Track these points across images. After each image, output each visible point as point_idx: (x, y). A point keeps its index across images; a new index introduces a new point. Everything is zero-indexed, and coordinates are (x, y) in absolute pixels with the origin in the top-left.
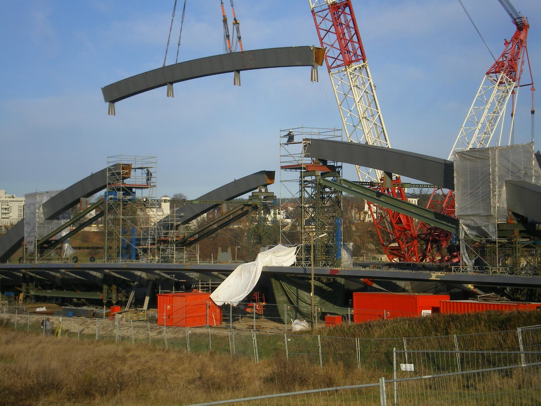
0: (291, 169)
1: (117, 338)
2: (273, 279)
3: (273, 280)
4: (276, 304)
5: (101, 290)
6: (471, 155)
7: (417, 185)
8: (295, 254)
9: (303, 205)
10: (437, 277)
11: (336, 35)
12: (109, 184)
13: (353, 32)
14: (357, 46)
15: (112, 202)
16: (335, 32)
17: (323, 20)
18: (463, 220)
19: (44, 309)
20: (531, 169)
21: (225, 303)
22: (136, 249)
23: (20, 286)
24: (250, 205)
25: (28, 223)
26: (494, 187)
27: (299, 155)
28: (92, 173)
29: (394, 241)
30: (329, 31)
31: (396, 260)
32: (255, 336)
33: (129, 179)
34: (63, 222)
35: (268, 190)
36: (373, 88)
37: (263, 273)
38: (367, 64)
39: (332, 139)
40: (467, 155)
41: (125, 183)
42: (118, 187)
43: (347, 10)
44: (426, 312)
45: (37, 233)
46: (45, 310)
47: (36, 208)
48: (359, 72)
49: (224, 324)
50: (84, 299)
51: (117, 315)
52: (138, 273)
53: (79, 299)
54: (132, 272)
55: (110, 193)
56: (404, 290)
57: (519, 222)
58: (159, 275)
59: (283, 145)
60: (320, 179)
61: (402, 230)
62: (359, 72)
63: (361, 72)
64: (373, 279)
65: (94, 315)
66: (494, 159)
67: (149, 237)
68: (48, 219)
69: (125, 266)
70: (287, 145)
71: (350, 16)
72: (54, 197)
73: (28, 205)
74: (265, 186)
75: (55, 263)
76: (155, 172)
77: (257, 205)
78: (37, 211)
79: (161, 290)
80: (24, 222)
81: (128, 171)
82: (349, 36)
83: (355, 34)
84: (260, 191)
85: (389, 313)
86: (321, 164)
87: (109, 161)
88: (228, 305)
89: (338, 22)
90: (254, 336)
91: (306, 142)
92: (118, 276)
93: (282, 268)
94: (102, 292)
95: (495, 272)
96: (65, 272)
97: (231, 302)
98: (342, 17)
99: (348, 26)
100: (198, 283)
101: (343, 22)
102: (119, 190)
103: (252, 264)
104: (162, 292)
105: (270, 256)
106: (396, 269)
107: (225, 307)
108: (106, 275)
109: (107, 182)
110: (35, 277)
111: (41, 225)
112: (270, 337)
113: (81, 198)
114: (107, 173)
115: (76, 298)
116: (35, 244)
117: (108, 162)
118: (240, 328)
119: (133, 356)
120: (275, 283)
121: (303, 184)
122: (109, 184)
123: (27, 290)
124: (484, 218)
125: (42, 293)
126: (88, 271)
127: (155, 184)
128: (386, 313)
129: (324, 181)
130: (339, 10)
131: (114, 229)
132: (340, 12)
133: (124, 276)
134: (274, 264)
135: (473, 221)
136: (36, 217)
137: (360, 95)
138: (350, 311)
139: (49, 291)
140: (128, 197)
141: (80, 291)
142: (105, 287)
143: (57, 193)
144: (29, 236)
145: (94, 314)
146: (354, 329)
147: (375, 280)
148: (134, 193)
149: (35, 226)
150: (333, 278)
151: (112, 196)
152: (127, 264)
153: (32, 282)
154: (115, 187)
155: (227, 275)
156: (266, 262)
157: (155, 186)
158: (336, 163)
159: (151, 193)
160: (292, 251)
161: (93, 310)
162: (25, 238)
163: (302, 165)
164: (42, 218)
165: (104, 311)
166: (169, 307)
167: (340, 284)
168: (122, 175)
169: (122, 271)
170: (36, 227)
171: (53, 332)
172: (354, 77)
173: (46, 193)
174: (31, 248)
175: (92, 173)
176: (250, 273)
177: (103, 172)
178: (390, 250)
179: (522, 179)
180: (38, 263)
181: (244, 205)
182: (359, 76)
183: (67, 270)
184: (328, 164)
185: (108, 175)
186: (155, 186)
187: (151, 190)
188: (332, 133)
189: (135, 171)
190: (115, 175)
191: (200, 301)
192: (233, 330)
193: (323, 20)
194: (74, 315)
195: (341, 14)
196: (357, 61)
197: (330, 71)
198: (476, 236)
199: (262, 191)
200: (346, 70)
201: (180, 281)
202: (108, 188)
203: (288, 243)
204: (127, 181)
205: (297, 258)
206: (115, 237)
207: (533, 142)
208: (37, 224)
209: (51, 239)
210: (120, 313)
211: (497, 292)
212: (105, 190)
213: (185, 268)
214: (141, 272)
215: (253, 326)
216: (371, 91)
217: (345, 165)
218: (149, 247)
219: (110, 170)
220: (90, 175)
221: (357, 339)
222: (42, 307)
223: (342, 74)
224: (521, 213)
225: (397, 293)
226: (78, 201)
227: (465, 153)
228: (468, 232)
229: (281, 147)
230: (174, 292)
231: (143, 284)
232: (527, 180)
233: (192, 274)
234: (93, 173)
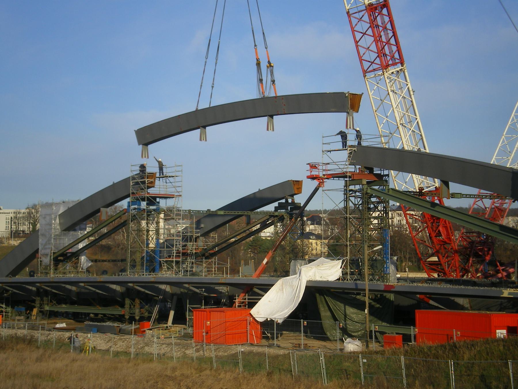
0: (334, 177)
1: (155, 356)
3: (317, 295)
4: (321, 320)
5: (122, 306)
7: (468, 195)
8: (341, 268)
9: (348, 215)
10: (510, 294)
11: (373, 38)
12: (133, 193)
13: (391, 34)
15: (136, 213)
16: (372, 35)
17: (359, 22)
19: (64, 325)
21: (267, 319)
22: (160, 261)
23: (34, 301)
24: (277, 216)
25: (43, 235)
27: (344, 163)
28: (114, 182)
29: (432, 255)
30: (365, 34)
31: (436, 275)
32: (323, 356)
33: (153, 188)
34: (80, 234)
35: (295, 200)
36: (412, 93)
37: (307, 288)
38: (405, 68)
39: (379, 146)
41: (149, 193)
42: (142, 197)
43: (385, 11)
44: (501, 333)
45: (53, 244)
46: (65, 326)
47: (52, 219)
48: (396, 76)
49: (264, 342)
50: (102, 314)
51: (147, 331)
52: (163, 287)
53: (96, 315)
54: (157, 285)
55: (133, 203)
56: (462, 308)
58: (188, 289)
59: (326, 152)
60: (367, 188)
61: (442, 243)
62: (396, 76)
63: (398, 77)
64: (431, 295)
65: (121, 332)
67: (174, 248)
68: (65, 230)
69: (153, 280)
70: (330, 152)
71: (388, 18)
72: (71, 207)
73: (43, 216)
74: (292, 196)
75: (71, 276)
76: (181, 181)
77: (283, 216)
78: (53, 222)
79: (189, 305)
80: (39, 234)
81: (153, 180)
82: (386, 39)
83: (393, 37)
85: (459, 333)
86: (367, 172)
87: (132, 170)
88: (272, 321)
89: (374, 24)
90: (321, 356)
91: (352, 149)
92: (143, 290)
93: (327, 282)
94: (124, 308)
96: (85, 286)
97: (275, 318)
98: (379, 19)
99: (385, 28)
100: (235, 298)
101: (380, 24)
102: (143, 200)
103: (296, 277)
104: (191, 307)
106: (451, 285)
107: (268, 324)
108: (128, 290)
109: (131, 191)
110: (51, 291)
112: (330, 356)
113: (102, 209)
114: (131, 182)
115: (93, 314)
116: (51, 256)
117: (131, 171)
118: (284, 346)
119: (183, 375)
120: (319, 298)
121: (347, 192)
122: (133, 193)
123: (41, 305)
125: (56, 310)
126: (107, 285)
127: (181, 194)
128: (456, 334)
129: (372, 190)
130: (376, 11)
131: (138, 240)
132: (377, 12)
133: (149, 291)
134: (318, 278)
136: (52, 228)
137: (397, 102)
138: (413, 331)
139: (64, 306)
140: (152, 207)
142: (128, 302)
143: (74, 204)
144: (46, 249)
145: (120, 330)
146: (435, 350)
147: (432, 296)
148: (159, 203)
149: (51, 238)
150: (380, 294)
151: (136, 206)
152: (155, 277)
153: (47, 296)
154: (140, 197)
155: (266, 291)
156: (310, 276)
157: (180, 196)
158: (382, 171)
159: (176, 203)
161: (119, 326)
162: (40, 250)
163: (347, 173)
164: (58, 229)
165: (133, 327)
166: (209, 323)
167: (388, 300)
168: (147, 183)
169: (147, 284)
170: (52, 239)
171: (81, 349)
172: (391, 81)
173: (63, 203)
174: (46, 260)
175: (114, 182)
176: (293, 288)
177: (126, 181)
178: (428, 265)
180: (52, 276)
181: (269, 216)
182: (396, 80)
183: (86, 284)
184: (374, 172)
185: (131, 184)
186: (180, 196)
187: (177, 200)
188: (379, 140)
189: (159, 180)
190: (140, 185)
191: (240, 317)
192: (278, 348)
193: (359, 22)
194: (97, 332)
195: (378, 15)
196: (394, 64)
197: (366, 76)
199: (289, 202)
200: (384, 74)
201: (211, 295)
202: (132, 198)
203: (332, 257)
204: (152, 191)
205: (342, 272)
206: (138, 249)
208: (53, 236)
209: (67, 251)
210: (151, 330)
212: (128, 200)
214: (166, 286)
215: (300, 345)
216: (409, 97)
217: (393, 173)
218: (174, 260)
219: (133, 178)
220: (112, 183)
221: (451, 361)
222: (62, 323)
223: (378, 78)
225: (466, 311)
226: (98, 211)
229: (323, 154)
230: (203, 307)
231: (167, 297)
233: (221, 288)
234: (115, 182)
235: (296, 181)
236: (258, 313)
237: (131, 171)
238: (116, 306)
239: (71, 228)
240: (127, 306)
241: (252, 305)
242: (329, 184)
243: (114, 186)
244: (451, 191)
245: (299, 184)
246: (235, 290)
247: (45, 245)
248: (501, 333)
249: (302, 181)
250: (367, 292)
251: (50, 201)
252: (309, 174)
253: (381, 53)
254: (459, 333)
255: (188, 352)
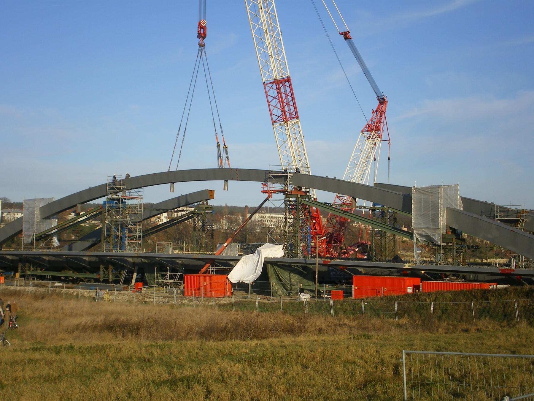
2: (270, 265)
6: (424, 190)
8: (283, 250)
10: (409, 266)
14: (292, 108)
18: (418, 231)
20: (457, 201)
21: (240, 282)
25: (26, 222)
26: (441, 211)
40: (423, 191)
52: (129, 259)
53: (67, 278)
57: (452, 233)
66: (441, 194)
68: (43, 219)
73: (27, 208)
74: (207, 200)
80: (23, 220)
84: (203, 204)
95: (440, 264)
105: (268, 251)
111: (39, 223)
113: (78, 205)
115: (63, 277)
117: (108, 180)
124: (432, 230)
134: (271, 256)
135: (424, 232)
136: (34, 217)
139: (39, 271)
141: (77, 272)
147: (348, 267)
156: (266, 255)
157: (142, 198)
160: (281, 247)
162: (23, 231)
179: (453, 206)
180: (34, 251)
185: (107, 189)
186: (142, 198)
198: (425, 241)
207: (458, 184)
208: (35, 222)
211: (458, 276)
213: (194, 257)
219: (109, 185)
220: (88, 188)
224: (456, 228)
226: (75, 206)
227: (421, 189)
228: (419, 238)
232: (454, 206)
234: (91, 187)
235: (210, 190)
236: (232, 277)
237: (108, 180)
238: (87, 272)
239: (48, 218)
240: (101, 272)
241: (228, 272)
242: (275, 196)
243: (90, 190)
244: (358, 204)
245: (211, 193)
246: (202, 263)
247: (29, 228)
248: (410, 290)
249: (214, 190)
250: (317, 264)
251: (34, 197)
252: (262, 189)
253: (284, 112)
254: (386, 289)
255: (183, 301)
